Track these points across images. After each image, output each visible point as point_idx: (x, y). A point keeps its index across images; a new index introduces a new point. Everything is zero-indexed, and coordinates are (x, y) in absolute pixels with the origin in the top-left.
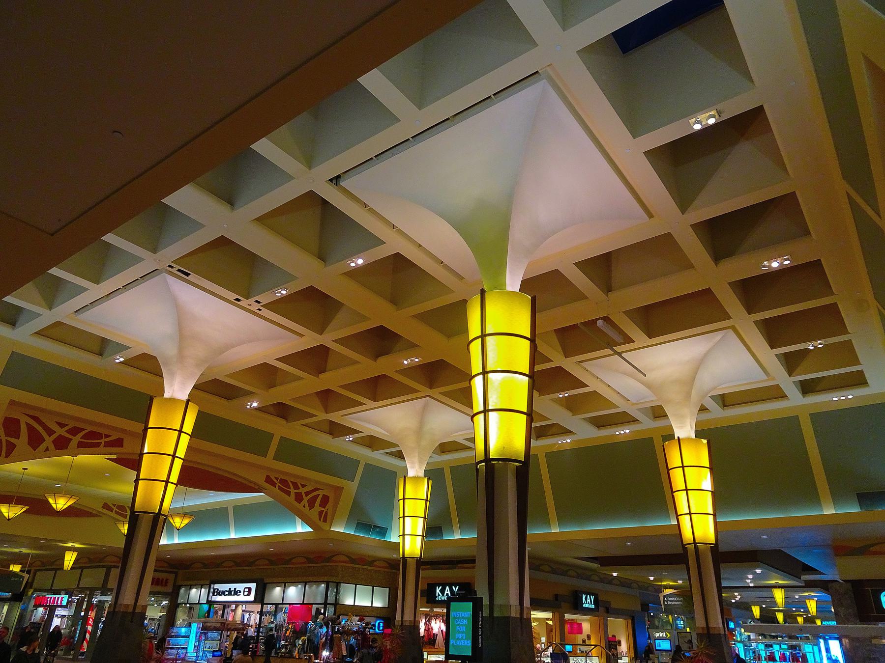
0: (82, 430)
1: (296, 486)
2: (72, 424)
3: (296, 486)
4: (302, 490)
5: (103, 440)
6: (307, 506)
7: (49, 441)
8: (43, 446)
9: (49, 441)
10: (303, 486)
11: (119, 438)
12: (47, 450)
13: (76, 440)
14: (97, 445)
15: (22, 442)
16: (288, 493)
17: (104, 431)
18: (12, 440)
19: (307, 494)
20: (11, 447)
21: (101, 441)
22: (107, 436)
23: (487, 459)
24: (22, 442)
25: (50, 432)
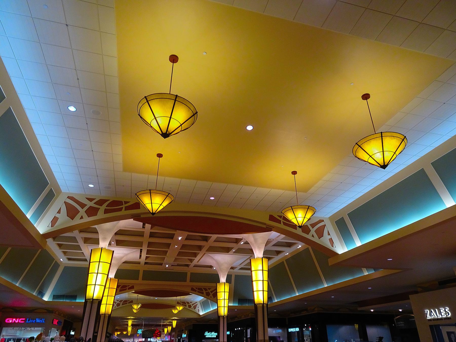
1: (206, 290)
3: (206, 290)
4: (209, 291)
6: (212, 297)
10: (209, 289)
11: (133, 286)
14: (126, 289)
16: (203, 293)
17: (127, 285)
19: (212, 292)
21: (126, 288)
22: (128, 286)
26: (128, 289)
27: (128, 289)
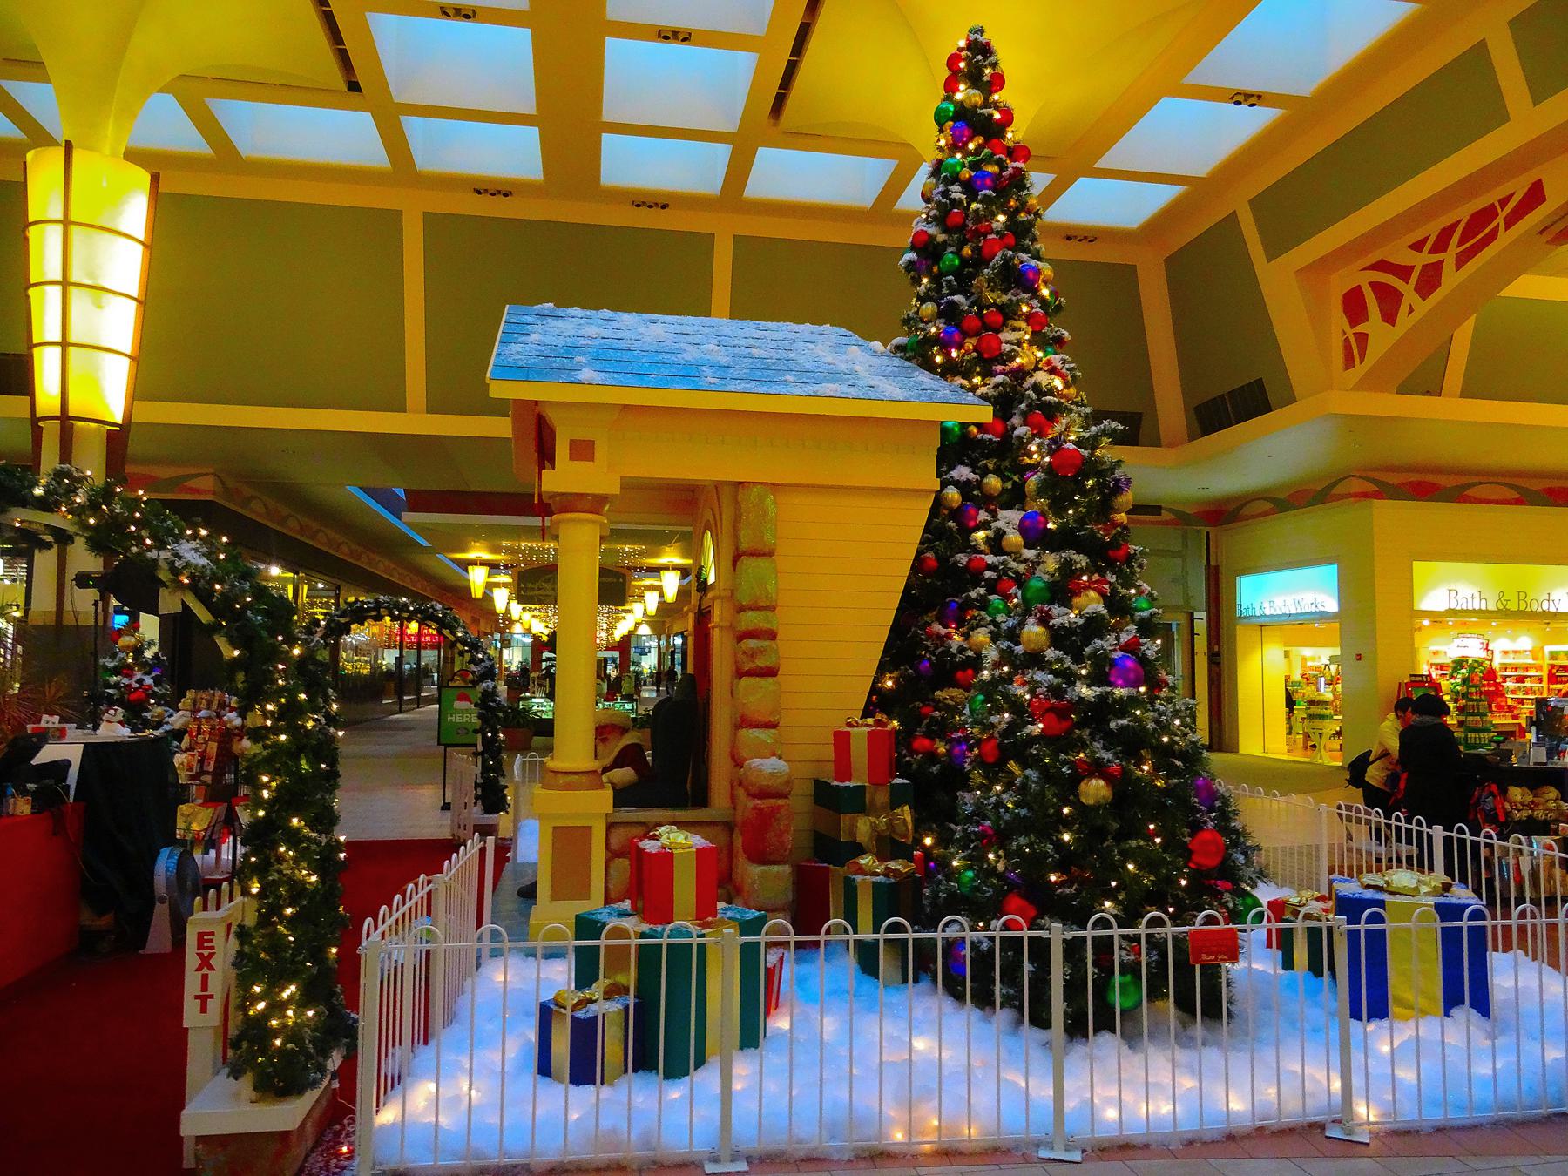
0: (1459, 221)
2: (1432, 229)
5: (1500, 220)
7: (1408, 289)
8: (1404, 308)
9: (1408, 289)
12: (1411, 310)
13: (1449, 257)
14: (1493, 236)
15: (1374, 324)
18: (1361, 328)
20: (1362, 338)
22: (1504, 202)
23: (65, 418)
24: (1374, 324)
25: (1404, 272)
26: (1507, 228)
27: (1507, 228)
